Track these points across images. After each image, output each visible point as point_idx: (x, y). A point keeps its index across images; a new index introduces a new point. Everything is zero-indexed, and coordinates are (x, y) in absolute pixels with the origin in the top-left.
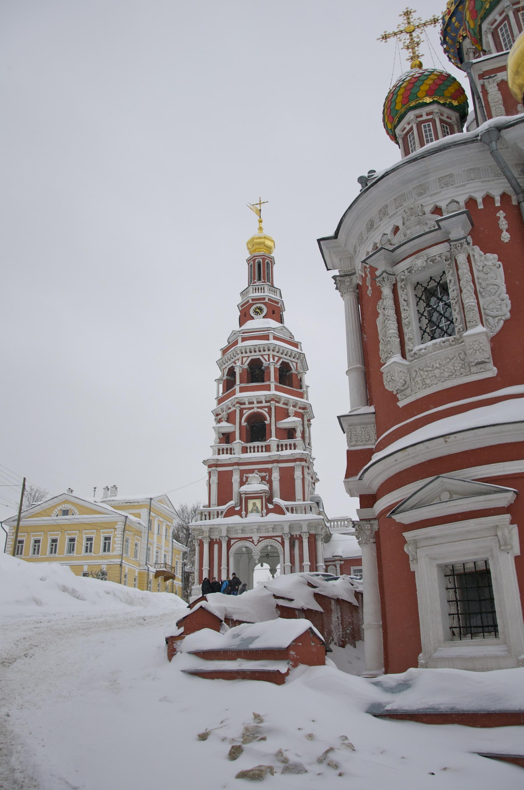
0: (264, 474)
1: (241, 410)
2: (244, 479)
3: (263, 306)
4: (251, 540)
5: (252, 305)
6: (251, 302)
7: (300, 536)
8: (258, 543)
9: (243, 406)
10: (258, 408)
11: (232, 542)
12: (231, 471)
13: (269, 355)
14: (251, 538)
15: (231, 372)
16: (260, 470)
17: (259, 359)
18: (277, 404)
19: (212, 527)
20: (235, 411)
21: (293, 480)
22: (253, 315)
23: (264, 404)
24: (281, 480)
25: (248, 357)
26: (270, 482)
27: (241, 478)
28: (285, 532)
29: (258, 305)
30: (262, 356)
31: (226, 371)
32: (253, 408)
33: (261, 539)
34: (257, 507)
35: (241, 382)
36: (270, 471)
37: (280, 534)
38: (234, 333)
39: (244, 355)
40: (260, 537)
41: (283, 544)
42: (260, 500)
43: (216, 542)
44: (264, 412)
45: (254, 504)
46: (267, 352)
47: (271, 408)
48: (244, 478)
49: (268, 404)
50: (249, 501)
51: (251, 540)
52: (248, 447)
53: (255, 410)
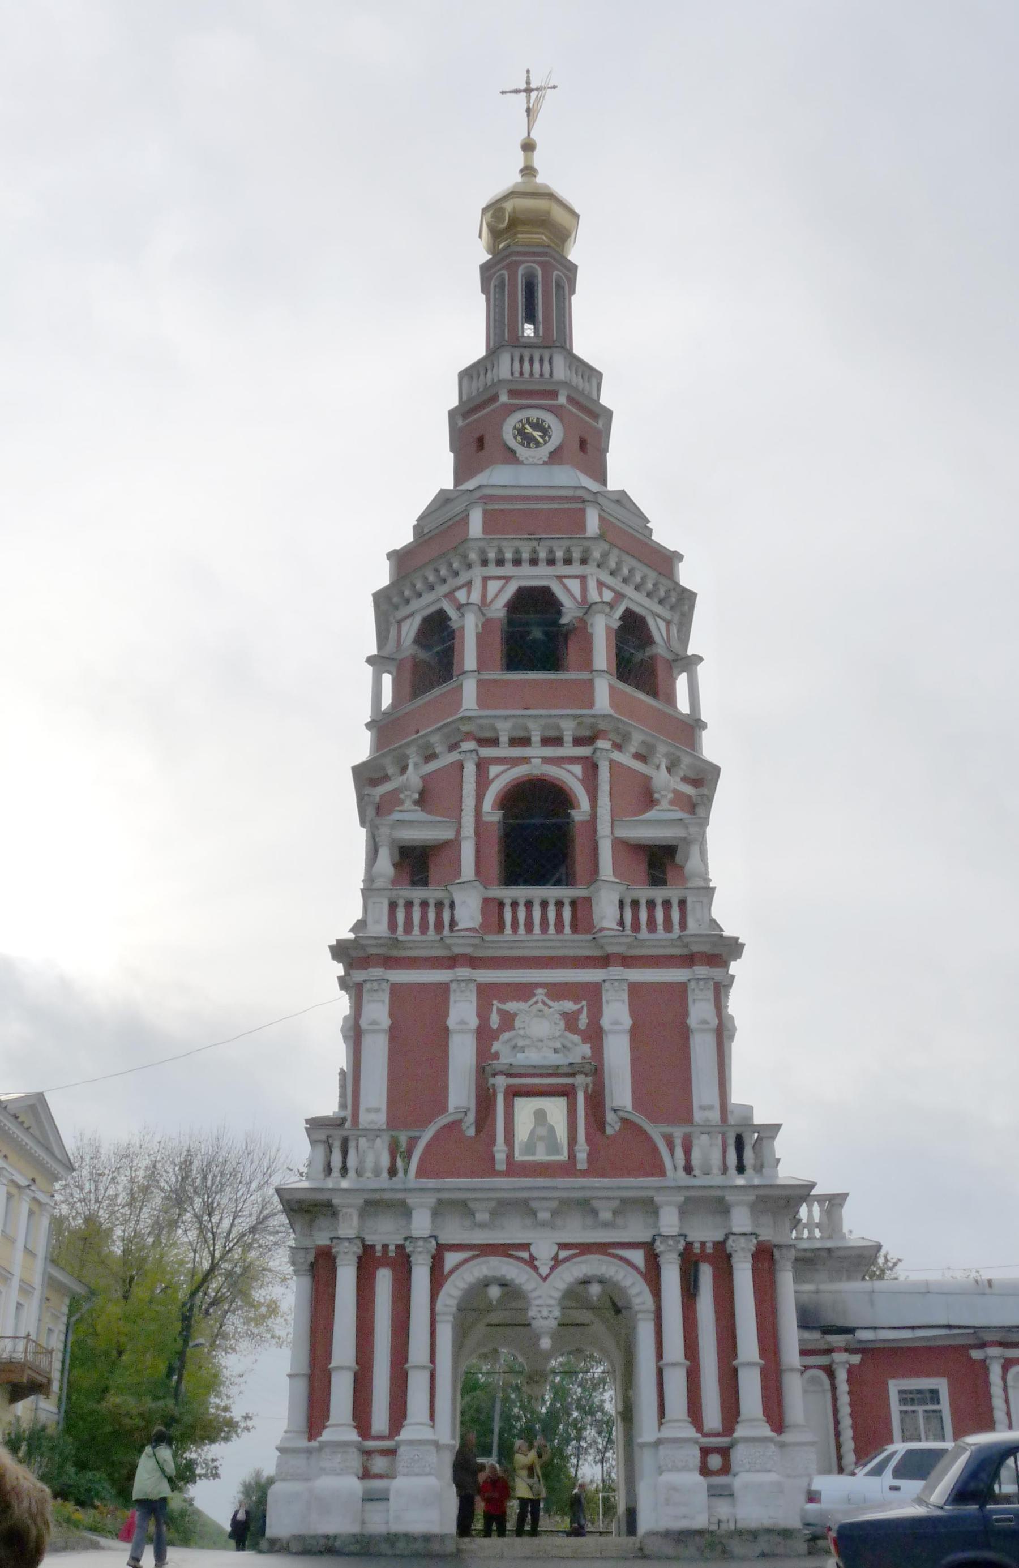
0: (569, 1006)
1: (482, 766)
2: (495, 1021)
3: (550, 420)
4: (525, 1255)
5: (510, 410)
6: (504, 398)
7: (720, 1246)
8: (553, 1269)
9: (487, 752)
10: (546, 760)
11: (451, 1259)
12: (444, 989)
13: (583, 579)
14: (526, 1246)
15: (438, 631)
16: (558, 991)
17: (546, 591)
18: (617, 756)
19: (377, 1196)
20: (460, 766)
21: (684, 1033)
22: (512, 443)
23: (569, 750)
24: (635, 1033)
25: (507, 579)
26: (595, 1035)
27: (483, 1014)
28: (665, 1231)
29: (534, 414)
30: (560, 578)
31: (410, 629)
32: (526, 760)
33: (563, 1254)
34: (552, 1130)
35: (482, 664)
36: (593, 994)
37: (645, 1237)
38: (443, 499)
39: (493, 570)
40: (563, 1246)
41: (653, 1275)
42: (561, 1102)
43: (384, 1261)
44: (571, 778)
45: (540, 1116)
46: (576, 569)
47: (595, 767)
48: (495, 1021)
49: (584, 751)
50: (520, 1102)
51: (525, 1255)
52: (508, 902)
53: (536, 768)
